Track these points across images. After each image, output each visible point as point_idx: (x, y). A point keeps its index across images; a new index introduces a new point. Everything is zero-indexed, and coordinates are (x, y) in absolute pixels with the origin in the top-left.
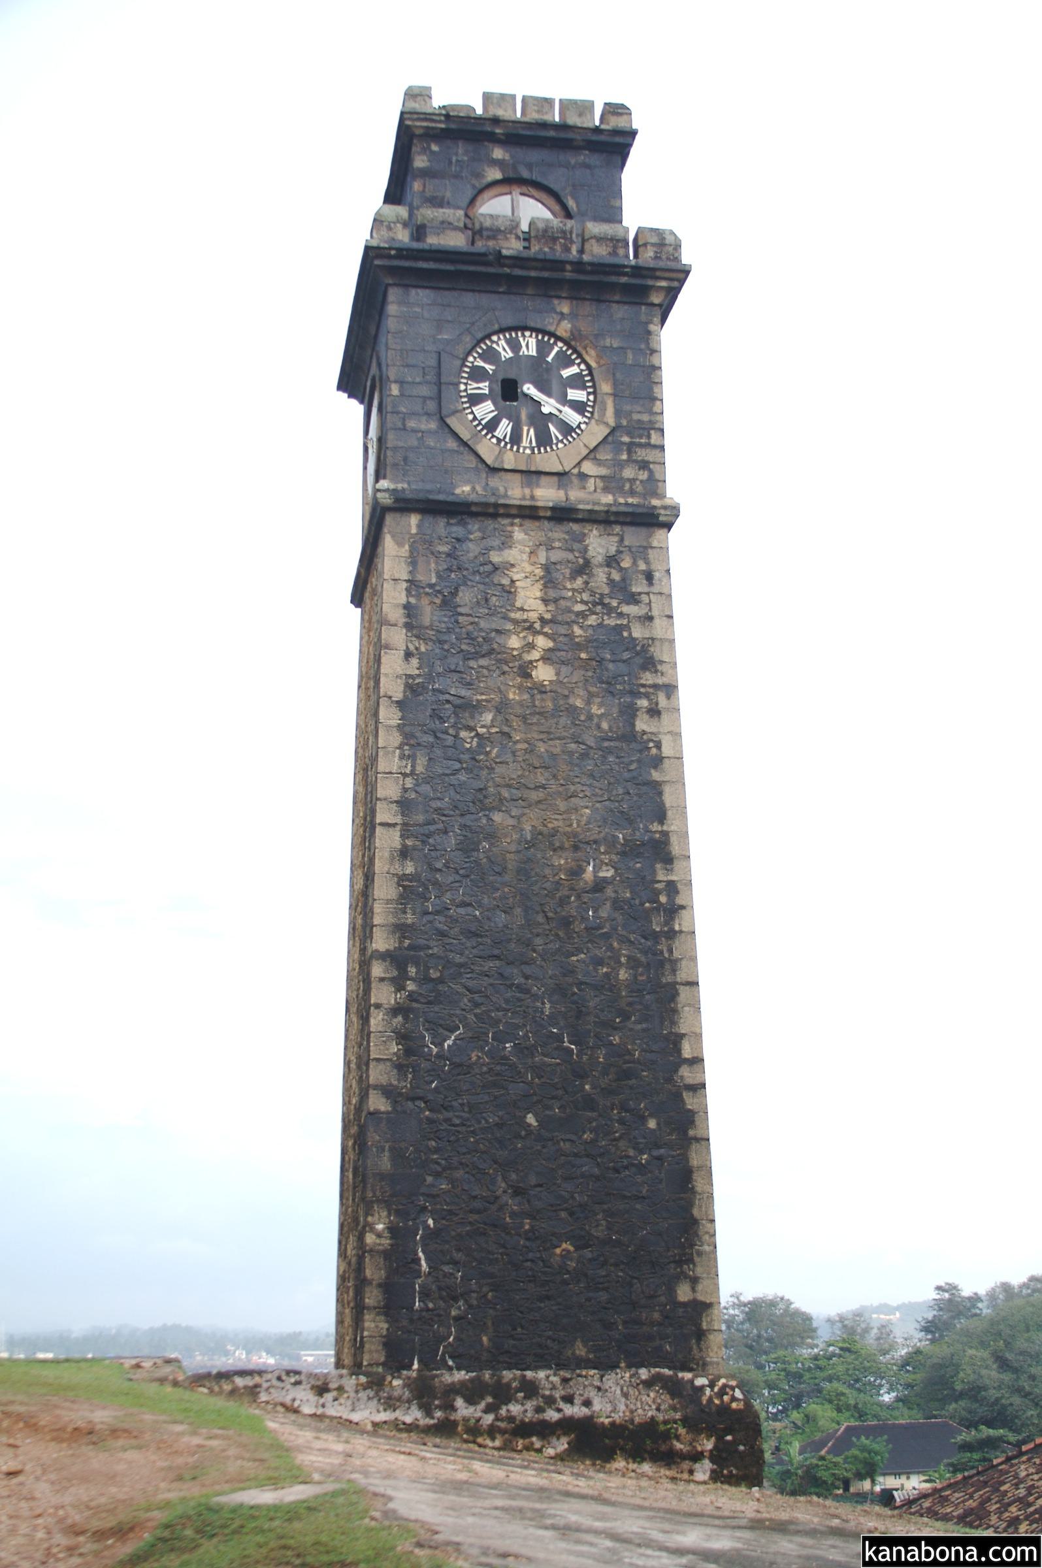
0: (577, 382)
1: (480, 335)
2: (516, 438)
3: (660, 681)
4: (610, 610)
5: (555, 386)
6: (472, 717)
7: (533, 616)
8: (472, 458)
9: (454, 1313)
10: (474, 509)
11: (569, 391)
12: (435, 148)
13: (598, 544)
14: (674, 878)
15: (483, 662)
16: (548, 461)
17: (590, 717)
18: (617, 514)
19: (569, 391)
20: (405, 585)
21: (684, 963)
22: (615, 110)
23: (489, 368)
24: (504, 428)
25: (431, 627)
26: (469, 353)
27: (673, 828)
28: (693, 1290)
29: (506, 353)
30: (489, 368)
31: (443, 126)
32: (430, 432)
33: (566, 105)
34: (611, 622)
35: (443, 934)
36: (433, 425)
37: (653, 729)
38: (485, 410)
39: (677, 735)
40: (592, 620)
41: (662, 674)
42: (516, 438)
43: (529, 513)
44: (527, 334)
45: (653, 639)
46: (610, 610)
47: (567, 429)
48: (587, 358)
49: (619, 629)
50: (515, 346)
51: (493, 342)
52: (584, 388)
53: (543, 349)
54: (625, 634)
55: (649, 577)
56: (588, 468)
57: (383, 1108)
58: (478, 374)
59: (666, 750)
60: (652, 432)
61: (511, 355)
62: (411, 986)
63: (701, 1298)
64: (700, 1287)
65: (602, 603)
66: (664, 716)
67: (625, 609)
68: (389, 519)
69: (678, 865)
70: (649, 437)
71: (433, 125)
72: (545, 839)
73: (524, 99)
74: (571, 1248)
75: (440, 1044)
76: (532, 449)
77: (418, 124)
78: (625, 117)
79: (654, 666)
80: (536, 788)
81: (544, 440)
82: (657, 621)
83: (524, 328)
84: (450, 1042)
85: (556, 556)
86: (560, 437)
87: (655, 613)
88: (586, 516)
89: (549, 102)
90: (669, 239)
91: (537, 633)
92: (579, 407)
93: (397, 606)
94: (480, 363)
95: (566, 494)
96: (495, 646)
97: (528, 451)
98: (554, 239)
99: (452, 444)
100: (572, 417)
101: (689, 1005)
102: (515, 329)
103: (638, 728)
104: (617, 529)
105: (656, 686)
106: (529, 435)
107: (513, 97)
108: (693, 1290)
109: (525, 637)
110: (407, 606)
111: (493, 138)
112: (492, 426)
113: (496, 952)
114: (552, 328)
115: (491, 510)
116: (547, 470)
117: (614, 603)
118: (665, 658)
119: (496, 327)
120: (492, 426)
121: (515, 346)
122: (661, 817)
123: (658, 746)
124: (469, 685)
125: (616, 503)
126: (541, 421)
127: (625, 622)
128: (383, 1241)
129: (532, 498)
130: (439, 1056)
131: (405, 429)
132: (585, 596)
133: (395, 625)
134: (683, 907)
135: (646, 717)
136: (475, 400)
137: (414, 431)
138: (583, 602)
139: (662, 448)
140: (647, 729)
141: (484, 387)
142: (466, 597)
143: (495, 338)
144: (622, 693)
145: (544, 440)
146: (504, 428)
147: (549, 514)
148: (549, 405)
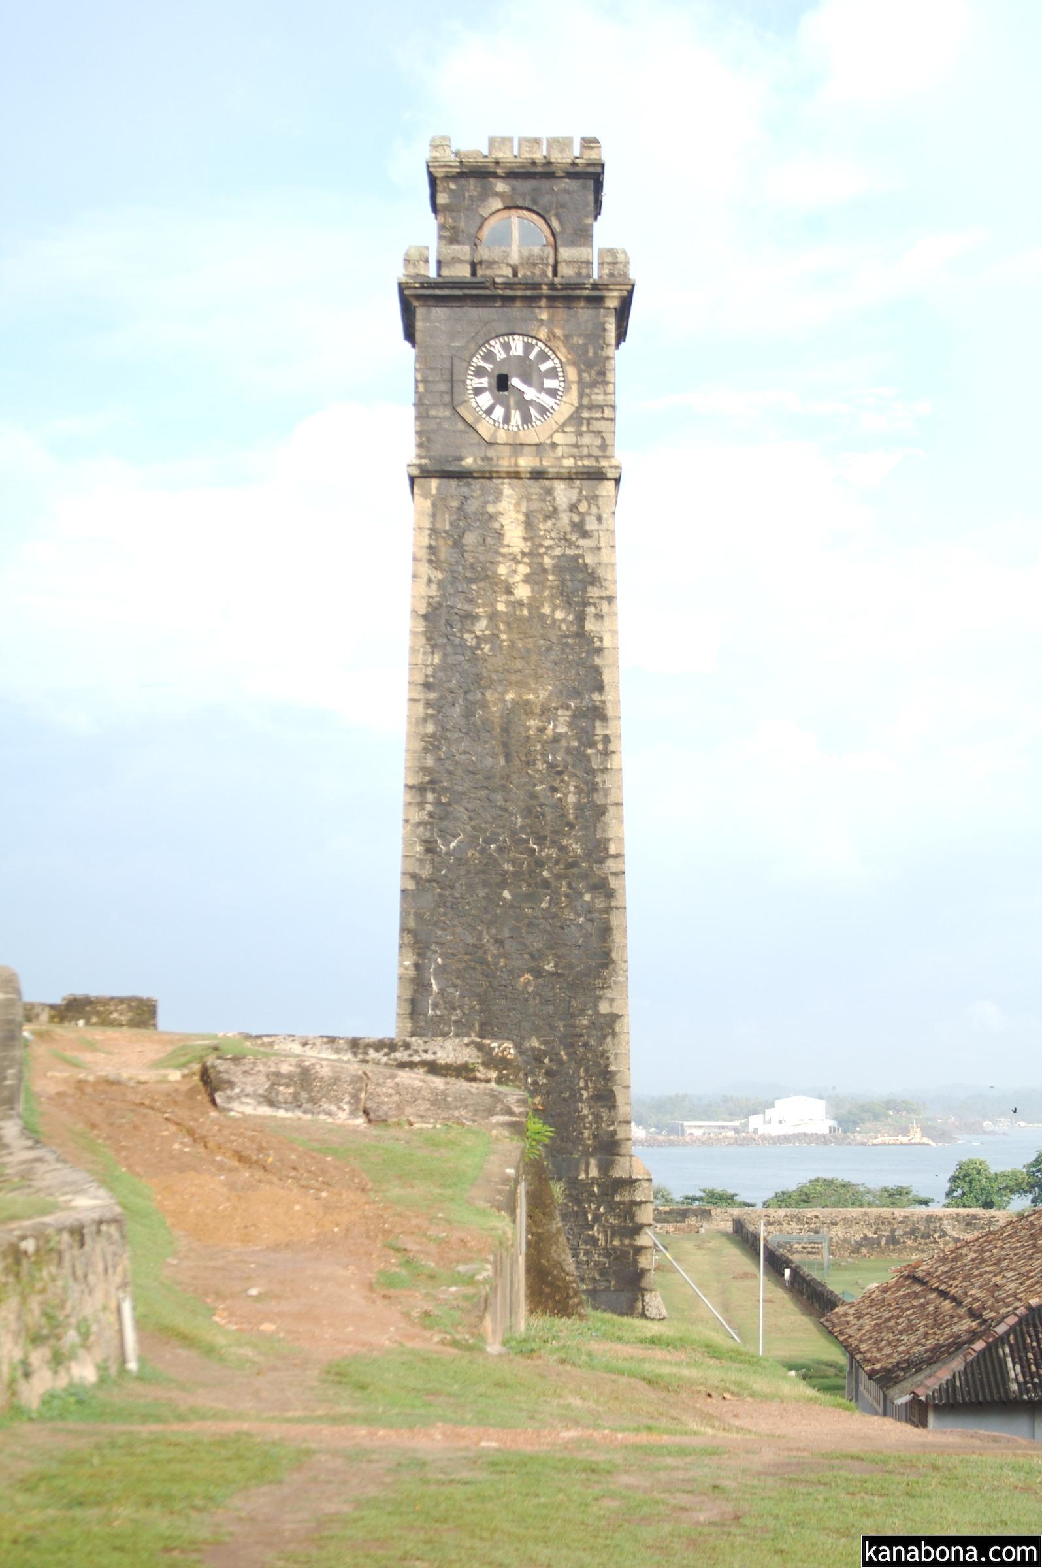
0: (552, 373)
1: (481, 342)
2: (507, 419)
3: (604, 594)
4: (570, 544)
5: (535, 378)
6: (473, 624)
7: (516, 550)
8: (475, 435)
9: (454, 1018)
10: (475, 475)
11: (545, 381)
12: (453, 186)
13: (563, 493)
14: (608, 732)
15: (482, 584)
16: (531, 435)
17: (554, 621)
18: (577, 473)
19: (545, 381)
20: (428, 532)
21: (613, 790)
22: (589, 143)
23: (489, 367)
24: (499, 412)
25: (446, 561)
26: (474, 355)
27: (609, 697)
28: (611, 1006)
29: (500, 355)
30: (489, 367)
31: (458, 170)
32: (446, 418)
33: (554, 142)
34: (570, 552)
35: (450, 773)
36: (448, 413)
37: (598, 629)
38: (486, 400)
39: (614, 632)
40: (558, 552)
41: (606, 588)
42: (507, 419)
43: (516, 475)
44: (516, 337)
45: (600, 564)
46: (570, 544)
47: (543, 410)
48: (559, 355)
49: (575, 558)
50: (506, 347)
51: (491, 346)
52: (557, 377)
53: (528, 348)
54: (581, 561)
55: (599, 519)
56: (559, 438)
57: (409, 887)
58: (480, 372)
59: (607, 643)
60: (605, 408)
61: (503, 356)
62: (429, 808)
63: (616, 1011)
64: (615, 1004)
65: (566, 540)
66: (606, 619)
67: (581, 542)
68: (417, 481)
69: (611, 723)
70: (603, 412)
71: (451, 170)
72: (525, 707)
73: (521, 140)
74: (531, 978)
75: (447, 844)
76: (518, 426)
77: (439, 169)
78: (596, 150)
79: (600, 583)
80: (516, 672)
81: (527, 419)
82: (604, 551)
83: (513, 334)
84: (452, 845)
85: (535, 505)
86: (539, 417)
87: (602, 544)
88: (555, 475)
89: (537, 141)
90: (621, 258)
91: (518, 562)
92: (553, 393)
93: (422, 547)
94: (482, 363)
95: (541, 461)
96: (489, 573)
97: (515, 429)
98: (535, 265)
99: (461, 426)
100: (547, 400)
101: (616, 818)
102: (507, 334)
103: (586, 629)
104: (578, 482)
105: (601, 598)
106: (516, 416)
107: (511, 140)
108: (611, 1006)
109: (510, 566)
110: (430, 547)
111: (495, 175)
112: (489, 411)
113: (486, 784)
114: (533, 333)
115: (487, 475)
116: (528, 442)
117: (574, 539)
118: (609, 577)
119: (493, 335)
120: (489, 411)
121: (506, 347)
122: (600, 688)
123: (601, 640)
124: (471, 601)
125: (577, 466)
126: (524, 406)
127: (580, 552)
128: (409, 972)
129: (516, 465)
130: (447, 853)
131: (428, 417)
132: (553, 535)
133: (421, 561)
134: (613, 752)
135: (593, 620)
136: (478, 391)
137: (435, 418)
138: (552, 539)
139: (613, 420)
140: (592, 628)
141: (484, 382)
142: (470, 539)
143: (492, 342)
144: (577, 604)
145: (527, 419)
146: (499, 412)
147: (528, 475)
148: (530, 393)
